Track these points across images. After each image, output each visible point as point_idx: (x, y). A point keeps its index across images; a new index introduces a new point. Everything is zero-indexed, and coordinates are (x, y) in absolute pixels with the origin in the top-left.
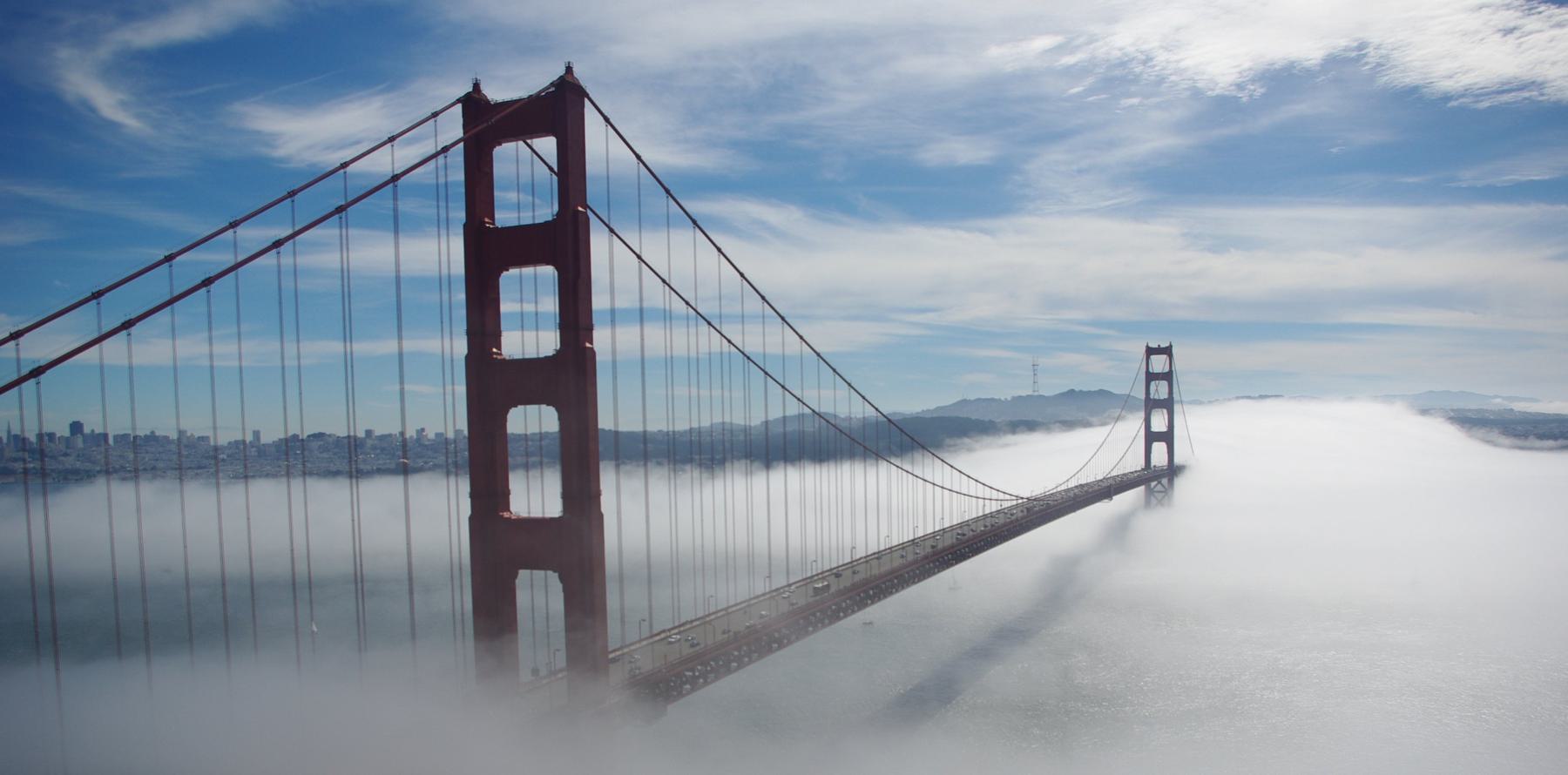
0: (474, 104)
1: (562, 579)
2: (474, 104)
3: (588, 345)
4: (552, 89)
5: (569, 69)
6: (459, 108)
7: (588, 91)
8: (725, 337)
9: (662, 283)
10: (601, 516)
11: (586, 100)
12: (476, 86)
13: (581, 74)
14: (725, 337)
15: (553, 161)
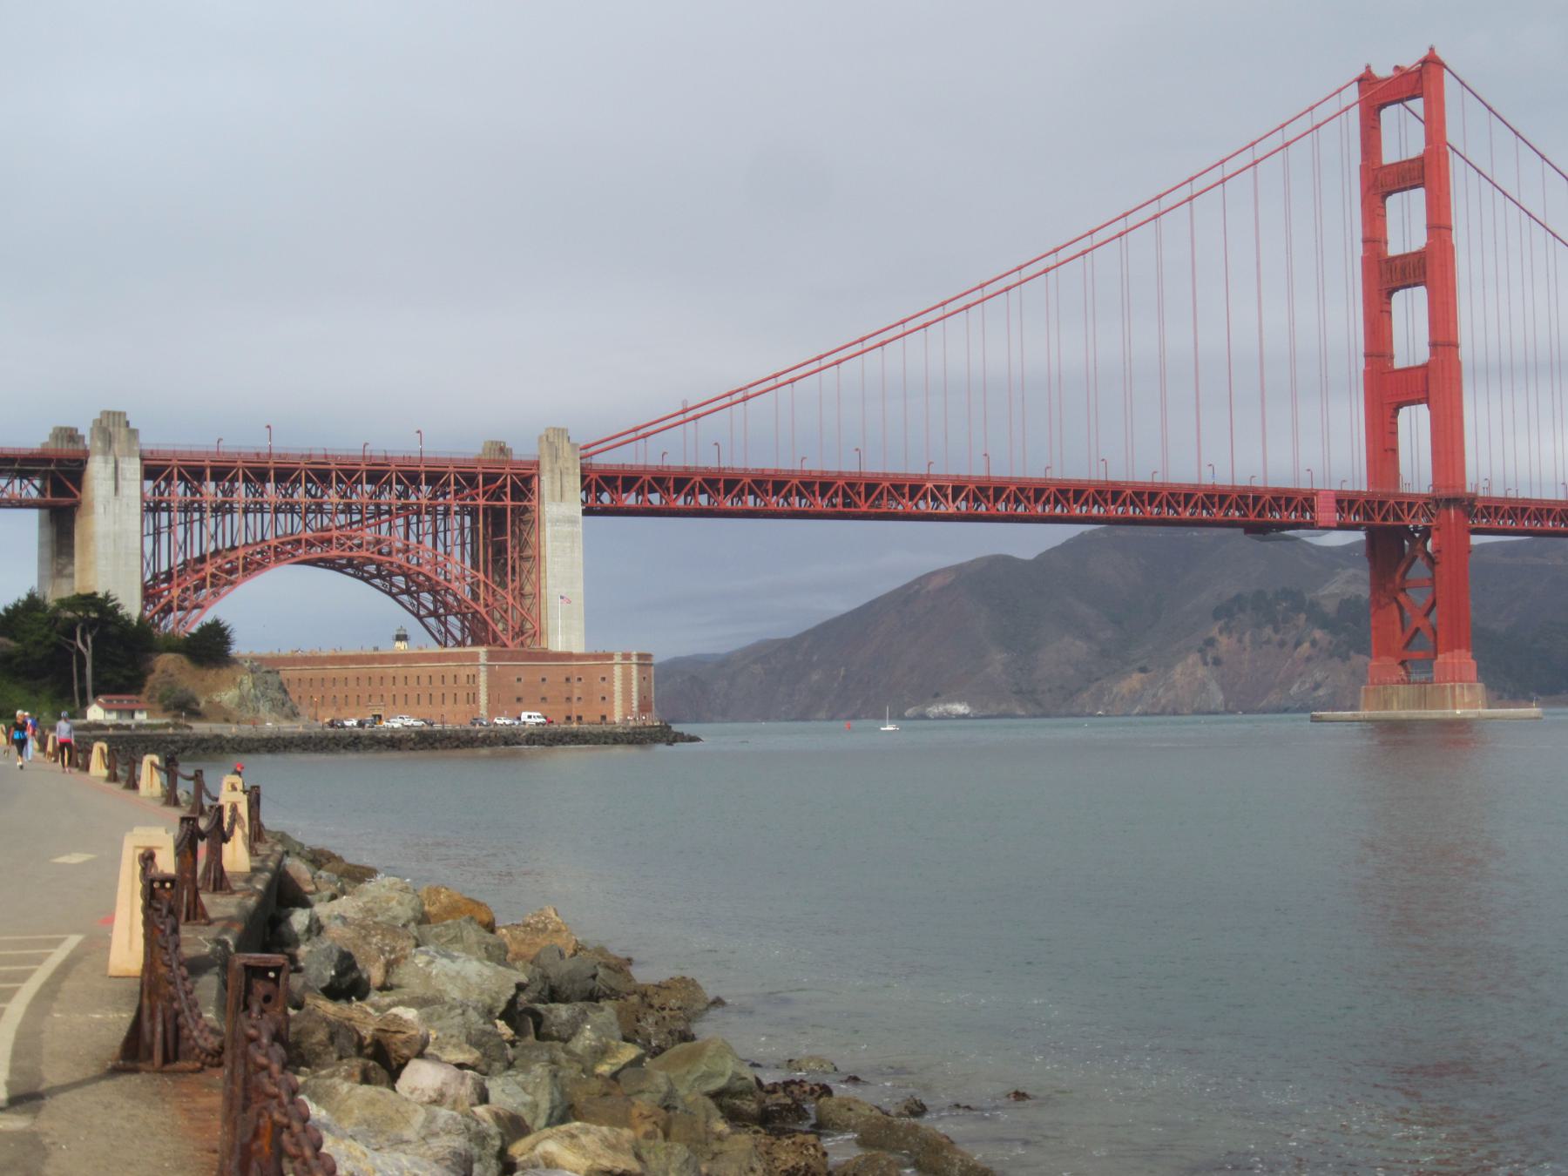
0: (1366, 80)
1: (1428, 406)
2: (1366, 80)
3: (1447, 238)
4: (1420, 65)
5: (1432, 49)
6: (1356, 83)
7: (1446, 63)
8: (1550, 231)
9: (1503, 196)
10: (1459, 363)
11: (1445, 70)
12: (1368, 67)
13: (1441, 54)
14: (1550, 231)
15: (1421, 114)
